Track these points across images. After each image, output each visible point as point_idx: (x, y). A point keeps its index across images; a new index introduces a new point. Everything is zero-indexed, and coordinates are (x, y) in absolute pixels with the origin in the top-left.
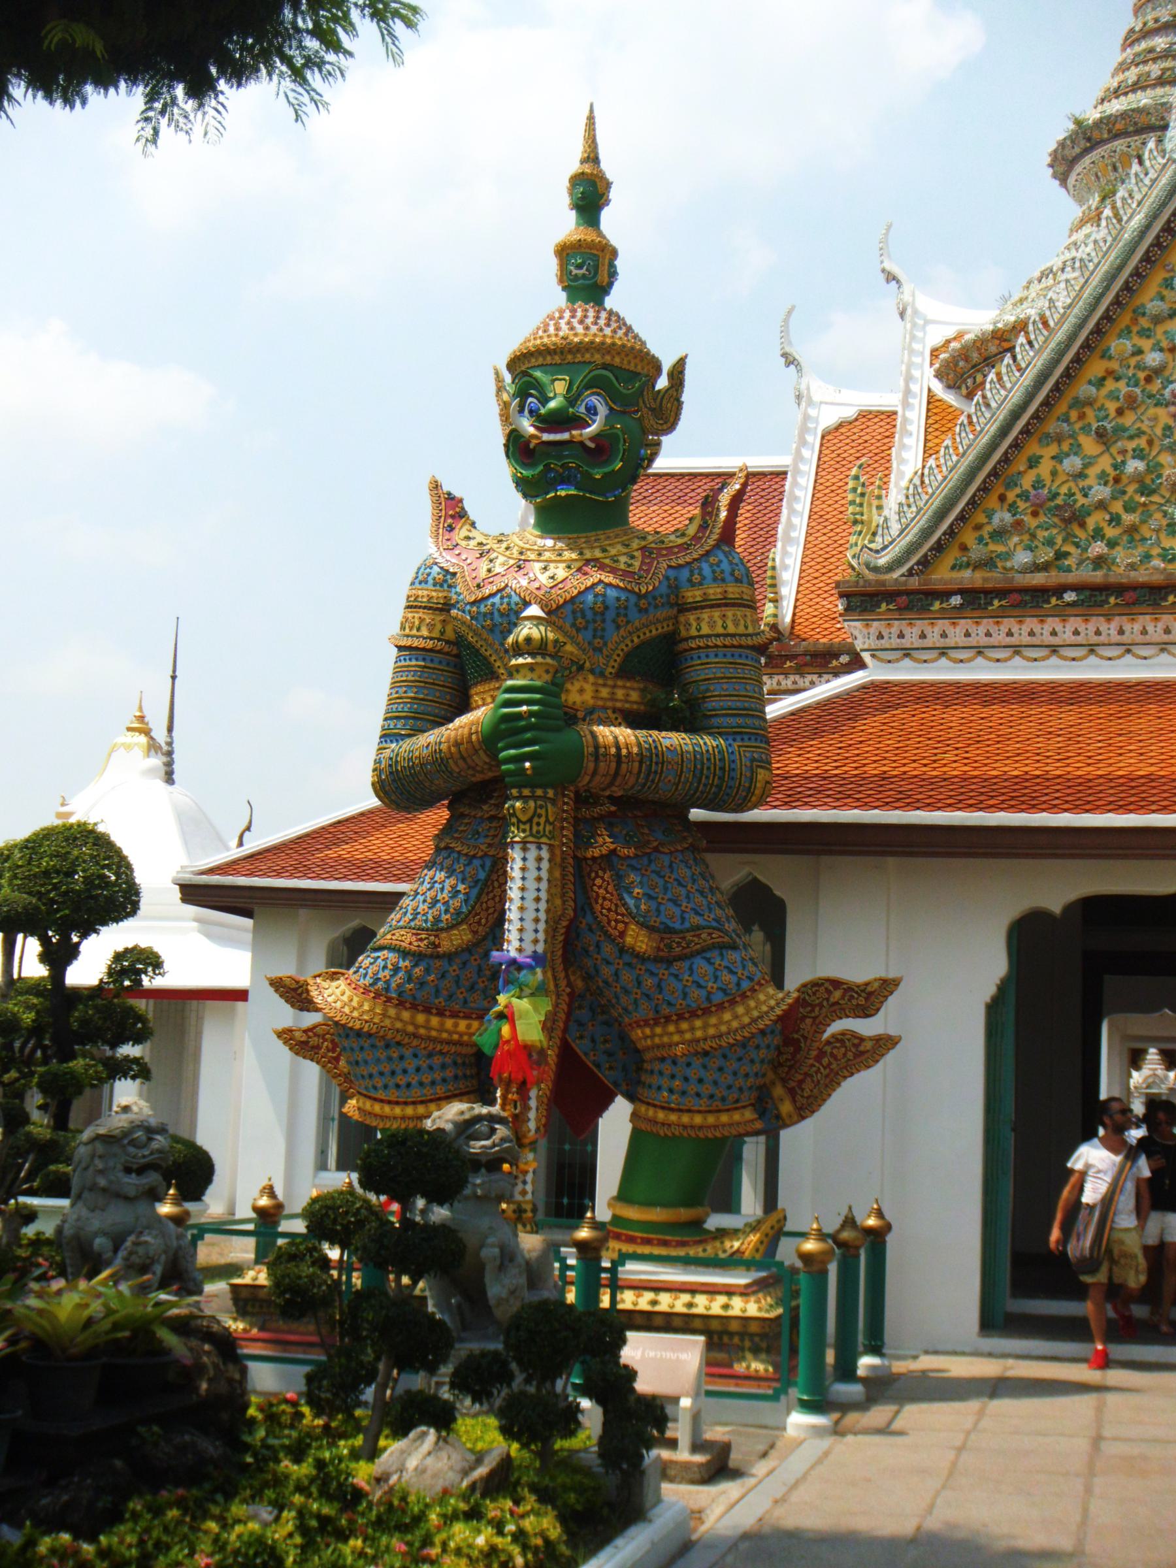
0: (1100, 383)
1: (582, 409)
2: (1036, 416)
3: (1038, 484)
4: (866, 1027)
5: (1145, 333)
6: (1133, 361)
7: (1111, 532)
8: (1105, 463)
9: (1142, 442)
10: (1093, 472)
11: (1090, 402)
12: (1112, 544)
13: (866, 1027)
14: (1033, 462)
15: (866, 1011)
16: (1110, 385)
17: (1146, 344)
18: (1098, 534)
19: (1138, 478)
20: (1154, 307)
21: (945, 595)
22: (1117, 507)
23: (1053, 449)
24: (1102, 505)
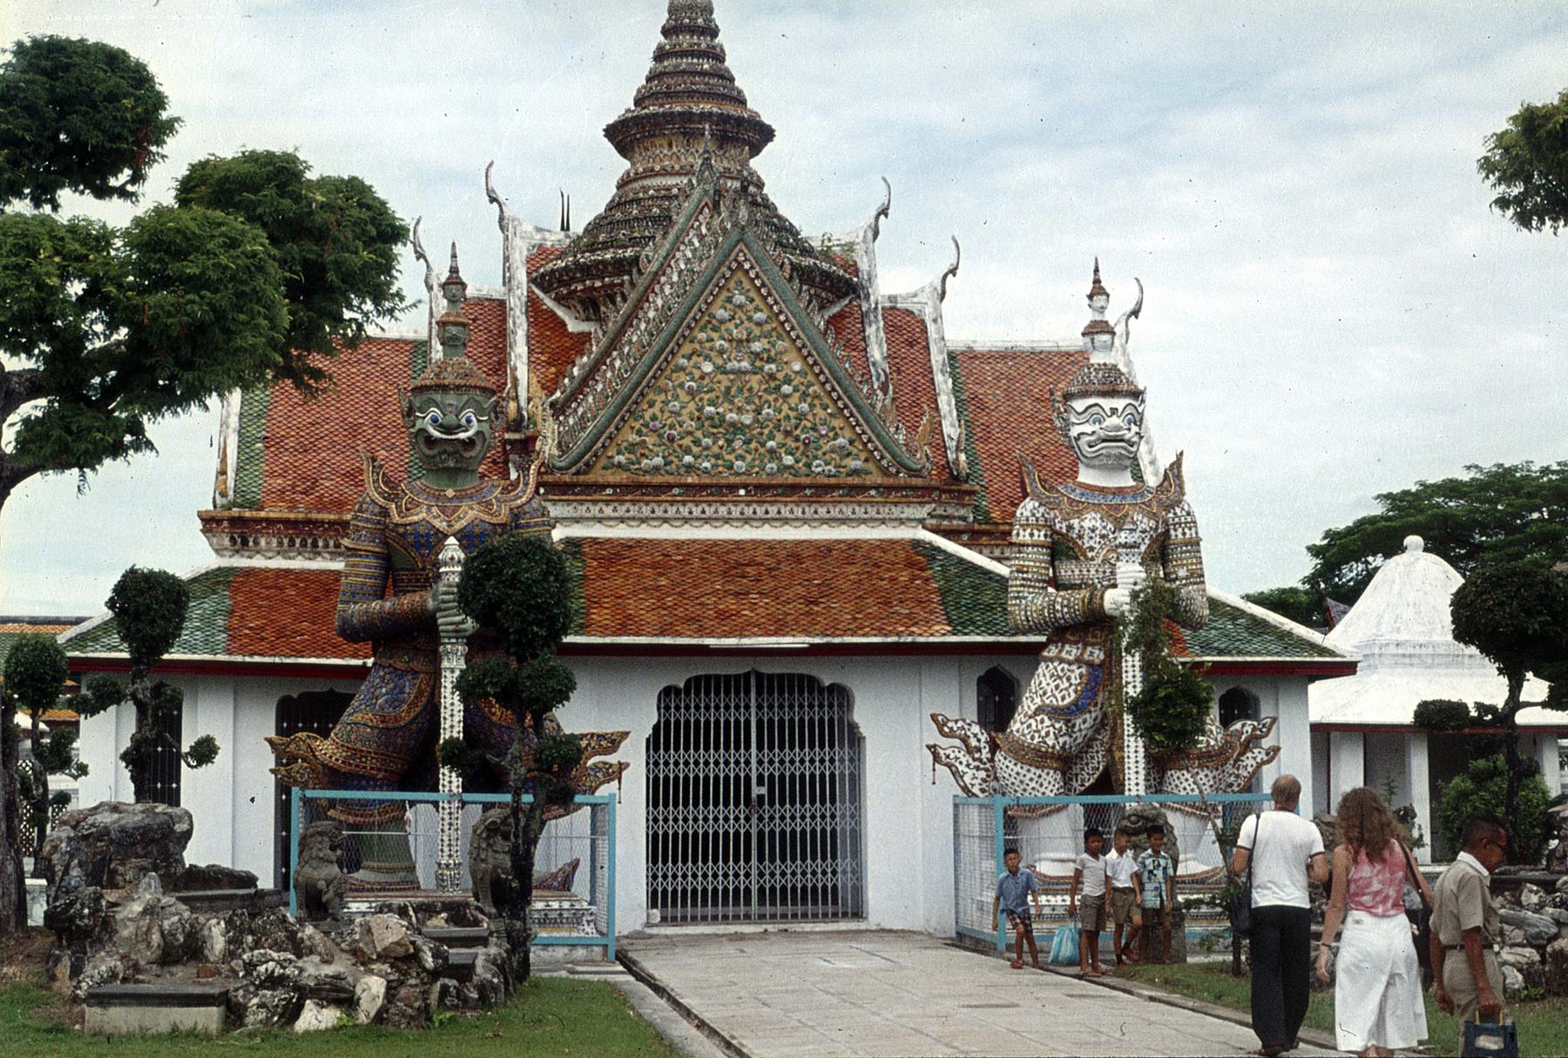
0: (689, 358)
1: (463, 421)
2: (654, 377)
3: (654, 418)
4: (612, 759)
5: (715, 329)
6: (708, 345)
7: (695, 450)
8: (692, 406)
9: (713, 395)
10: (684, 412)
11: (683, 369)
12: (696, 457)
13: (612, 759)
14: (651, 405)
15: (607, 751)
16: (695, 358)
17: (715, 335)
18: (688, 451)
19: (711, 418)
20: (721, 313)
21: (604, 487)
22: (699, 434)
23: (662, 397)
24: (691, 433)
